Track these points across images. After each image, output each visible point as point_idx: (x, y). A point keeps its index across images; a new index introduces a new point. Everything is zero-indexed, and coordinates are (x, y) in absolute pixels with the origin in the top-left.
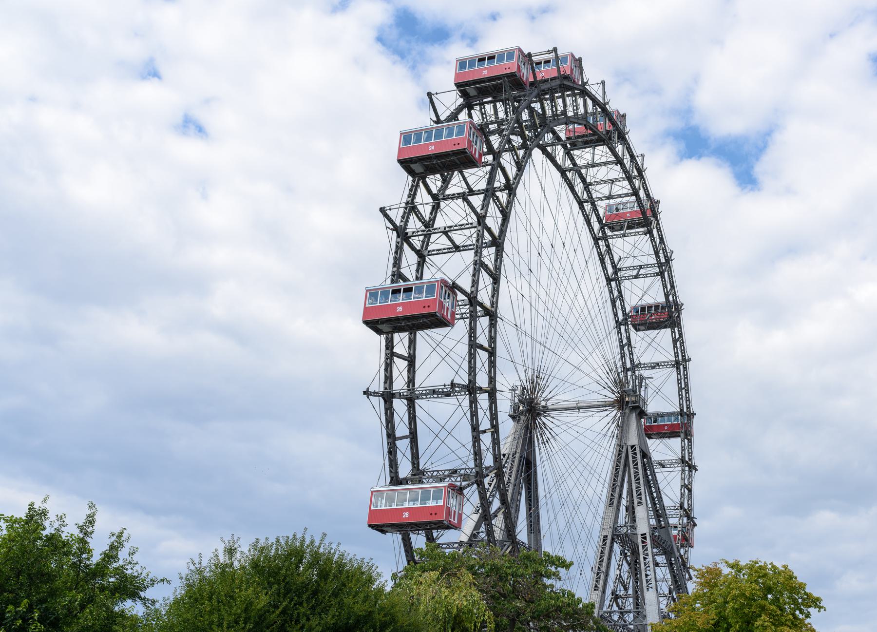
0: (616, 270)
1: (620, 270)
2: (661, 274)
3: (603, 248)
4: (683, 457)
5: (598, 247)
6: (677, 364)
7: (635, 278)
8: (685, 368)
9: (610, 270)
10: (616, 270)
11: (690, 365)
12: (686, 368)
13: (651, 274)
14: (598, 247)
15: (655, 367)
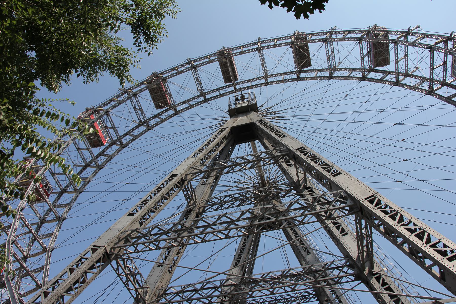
0: (141, 123)
1: (141, 121)
2: (135, 95)
3: (129, 138)
4: (257, 49)
5: (128, 143)
6: (194, 68)
7: (143, 112)
8: (195, 61)
9: (142, 128)
10: (141, 123)
11: (192, 57)
12: (195, 60)
13: (137, 102)
14: (128, 143)
15: (199, 81)
